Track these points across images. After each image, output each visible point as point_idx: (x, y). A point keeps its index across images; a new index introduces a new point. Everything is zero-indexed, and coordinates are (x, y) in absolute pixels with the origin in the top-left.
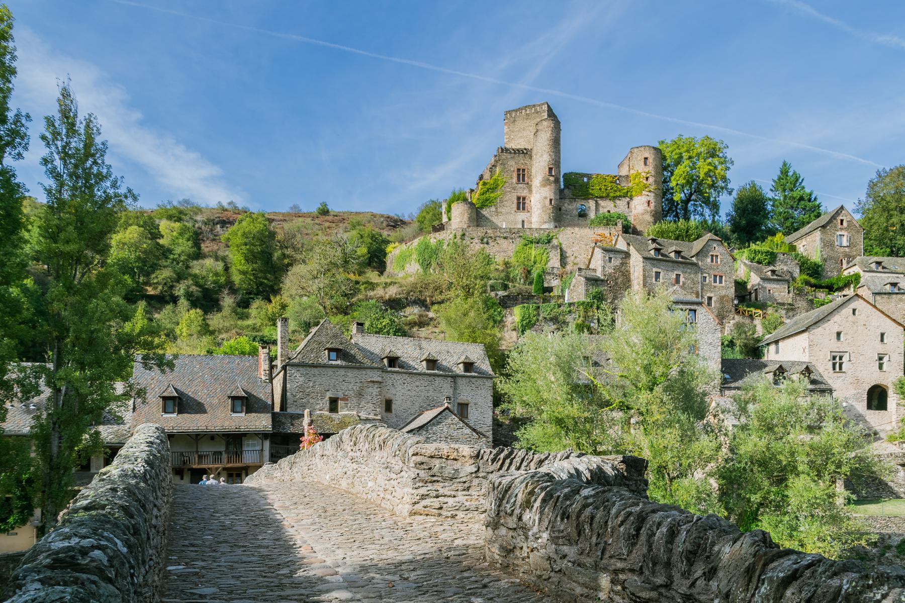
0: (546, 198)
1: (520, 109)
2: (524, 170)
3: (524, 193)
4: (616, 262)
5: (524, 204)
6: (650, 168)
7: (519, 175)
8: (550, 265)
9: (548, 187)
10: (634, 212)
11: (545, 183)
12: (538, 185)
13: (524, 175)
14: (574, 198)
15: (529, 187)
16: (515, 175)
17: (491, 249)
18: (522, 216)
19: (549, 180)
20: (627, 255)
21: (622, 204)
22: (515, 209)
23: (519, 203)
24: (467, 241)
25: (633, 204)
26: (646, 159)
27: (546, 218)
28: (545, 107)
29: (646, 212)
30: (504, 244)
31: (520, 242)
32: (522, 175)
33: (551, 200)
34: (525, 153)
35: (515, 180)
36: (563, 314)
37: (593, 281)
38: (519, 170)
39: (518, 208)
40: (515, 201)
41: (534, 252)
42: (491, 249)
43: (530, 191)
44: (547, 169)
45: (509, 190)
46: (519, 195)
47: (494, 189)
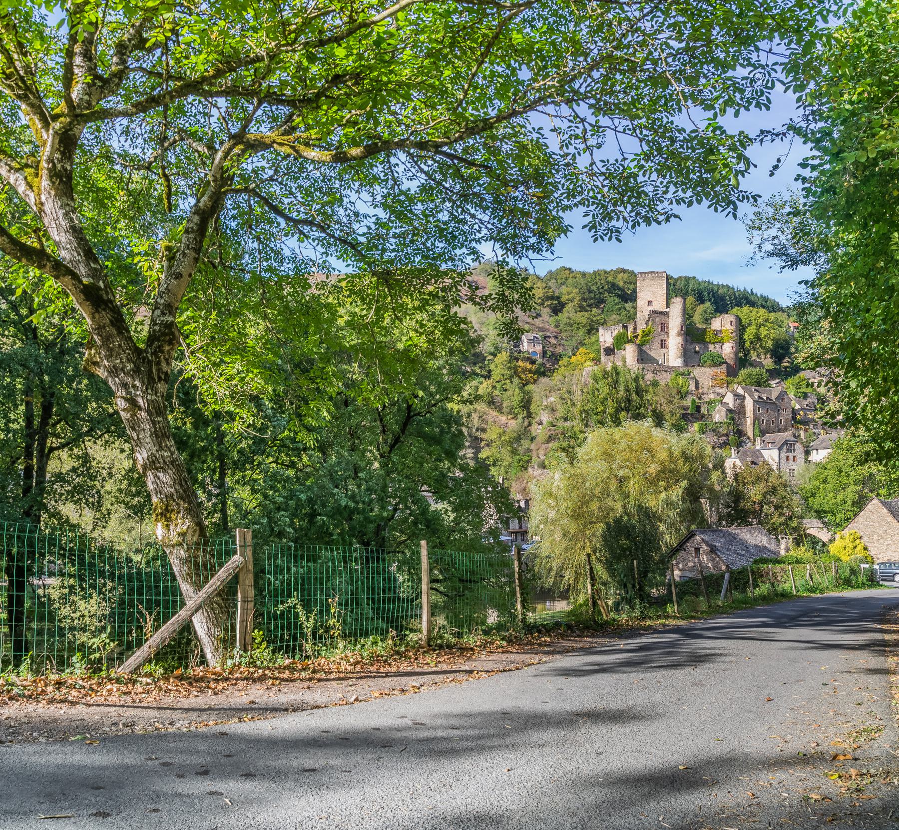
1: (648, 273)
3: (665, 338)
4: (739, 401)
6: (733, 327)
8: (690, 388)
10: (724, 352)
11: (679, 334)
14: (693, 342)
15: (667, 333)
17: (658, 378)
18: (663, 351)
20: (744, 397)
21: (718, 346)
24: (645, 372)
25: (724, 347)
27: (679, 355)
28: (664, 275)
29: (731, 353)
30: (665, 374)
31: (674, 374)
32: (664, 328)
34: (666, 314)
36: (717, 428)
37: (729, 411)
41: (681, 380)
42: (658, 378)
47: (648, 334)
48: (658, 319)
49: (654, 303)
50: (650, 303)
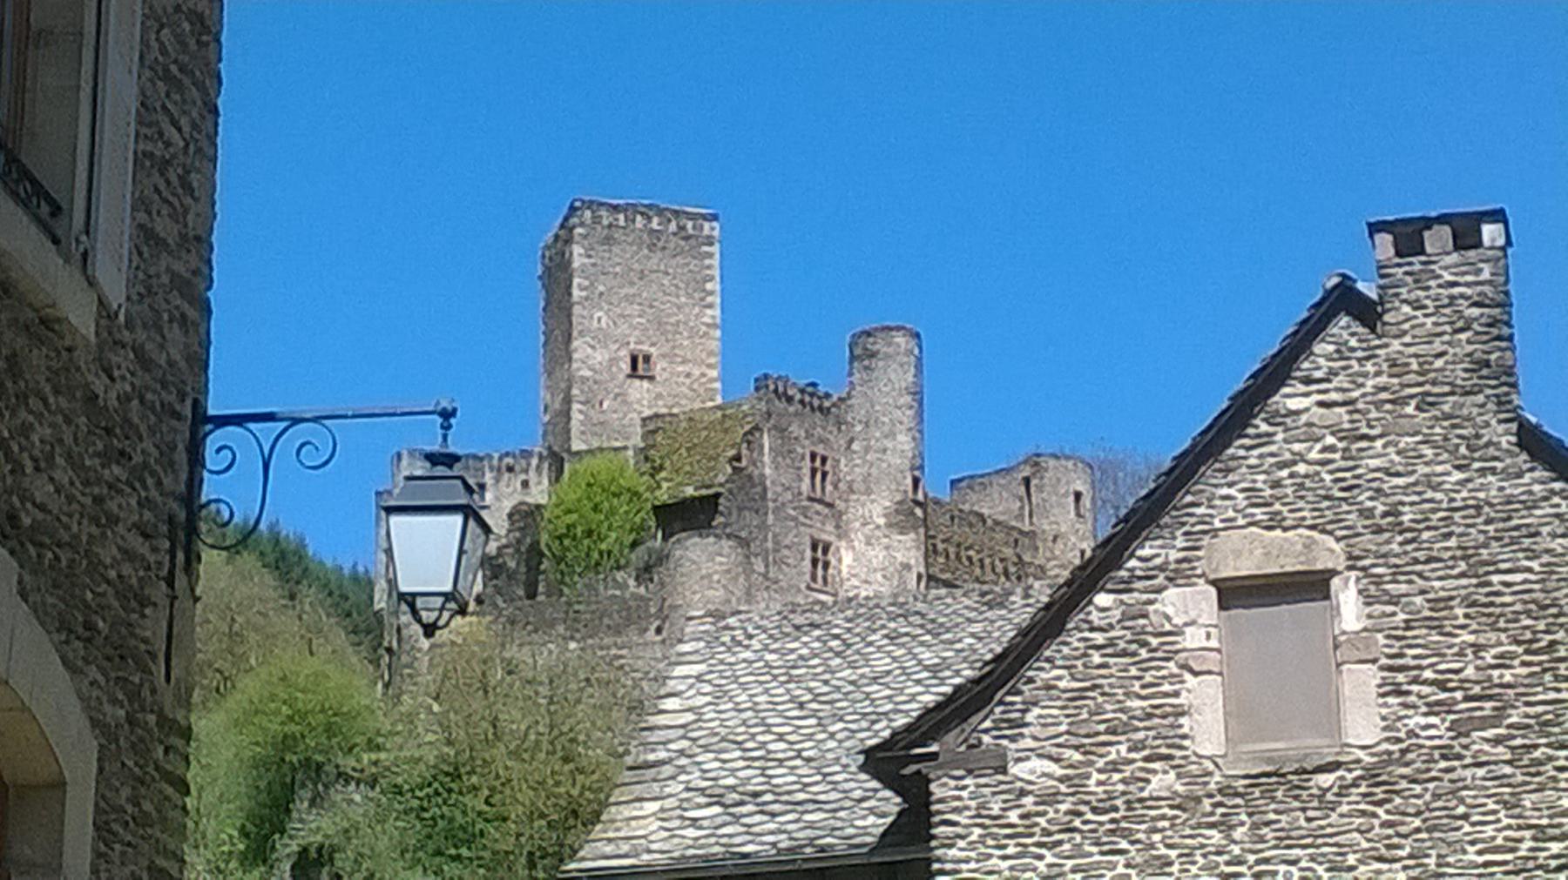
0: (907, 567)
2: (824, 460)
5: (826, 565)
7: (814, 471)
9: (912, 535)
12: (882, 521)
13: (824, 475)
16: (806, 471)
19: (913, 514)
22: (808, 577)
23: (815, 562)
26: (1078, 496)
33: (919, 577)
35: (805, 486)
38: (813, 456)
39: (814, 578)
40: (808, 554)
43: (842, 532)
44: (909, 481)
45: (792, 512)
46: (816, 536)
48: (795, 429)
49: (659, 367)
50: (638, 366)
